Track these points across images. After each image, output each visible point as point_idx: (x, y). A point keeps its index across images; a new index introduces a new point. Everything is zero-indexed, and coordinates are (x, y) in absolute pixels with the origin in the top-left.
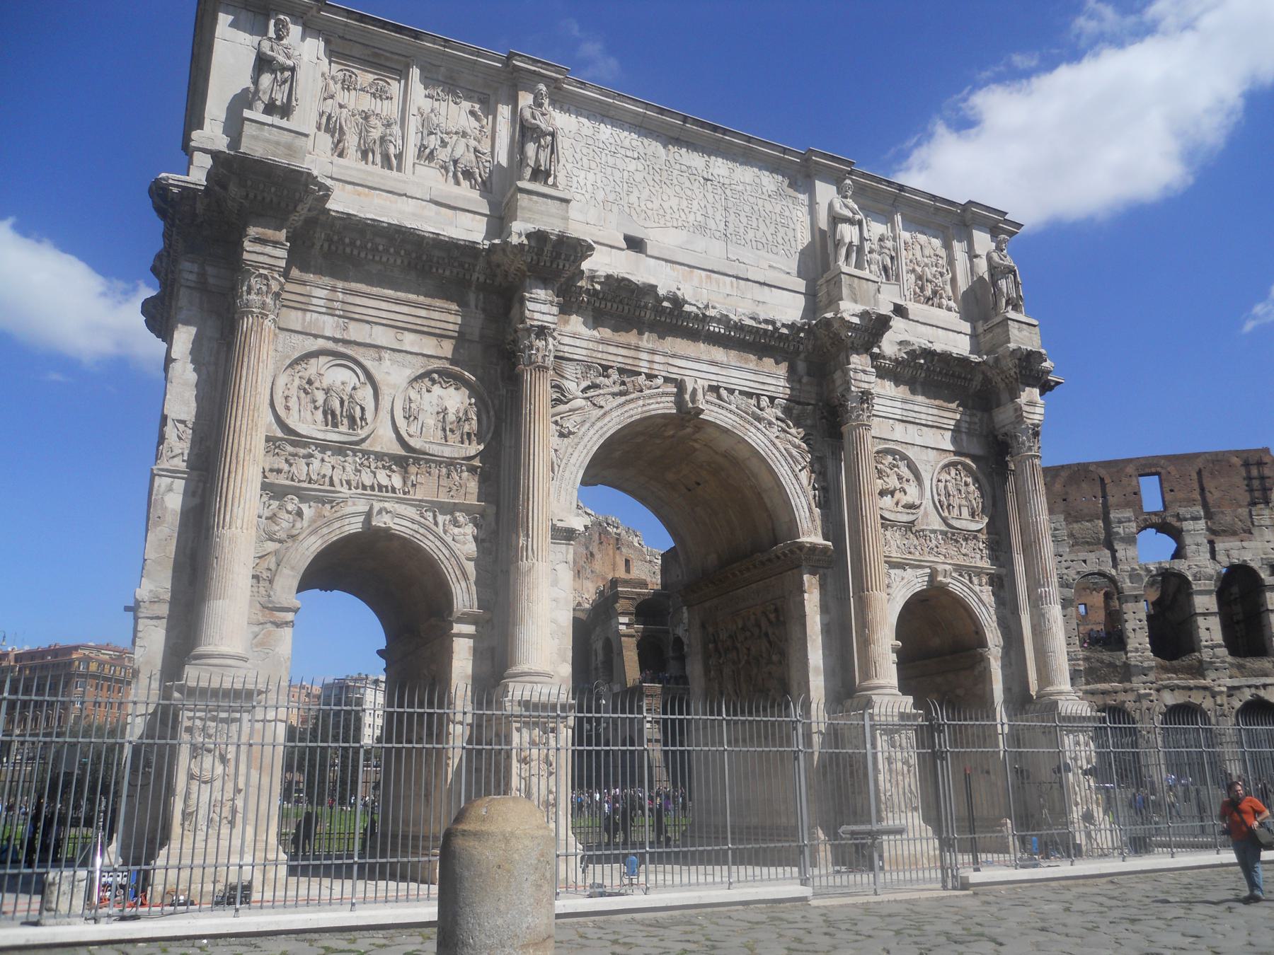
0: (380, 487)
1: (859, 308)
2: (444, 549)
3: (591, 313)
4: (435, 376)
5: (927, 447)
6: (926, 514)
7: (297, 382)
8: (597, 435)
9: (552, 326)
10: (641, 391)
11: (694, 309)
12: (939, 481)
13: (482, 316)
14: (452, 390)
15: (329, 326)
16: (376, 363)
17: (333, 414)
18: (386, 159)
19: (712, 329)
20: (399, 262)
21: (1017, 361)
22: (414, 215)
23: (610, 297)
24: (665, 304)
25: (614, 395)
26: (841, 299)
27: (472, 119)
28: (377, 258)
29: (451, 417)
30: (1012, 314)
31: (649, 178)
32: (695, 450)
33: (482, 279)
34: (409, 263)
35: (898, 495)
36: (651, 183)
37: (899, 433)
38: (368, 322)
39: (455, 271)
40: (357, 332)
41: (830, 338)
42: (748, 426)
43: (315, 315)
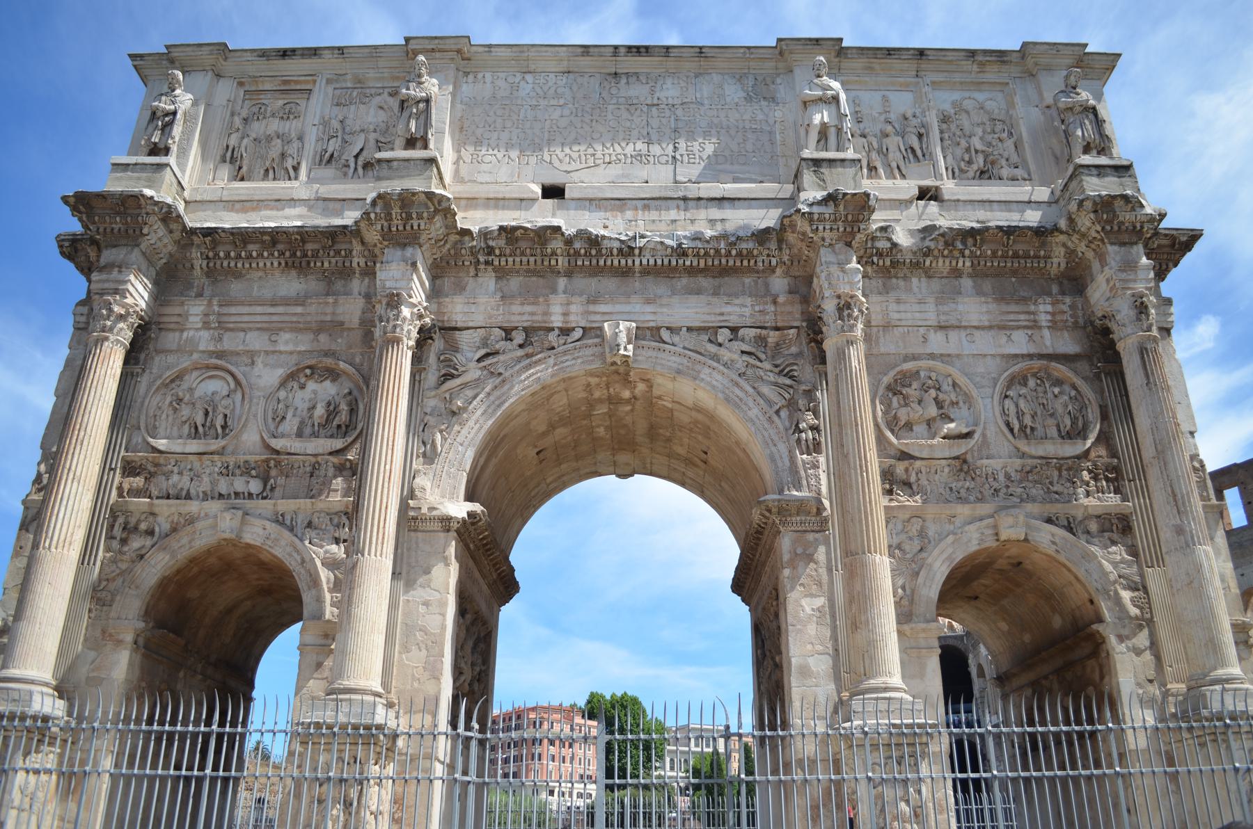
0: (237, 494)
1: (819, 195)
2: (295, 555)
3: (494, 274)
4: (308, 371)
5: (985, 355)
7: (169, 399)
8: (493, 407)
10: (553, 348)
11: (616, 245)
12: (1006, 397)
13: (364, 300)
14: (327, 383)
15: (204, 340)
16: (248, 369)
17: (196, 428)
19: (645, 262)
20: (276, 264)
21: (1092, 216)
23: (508, 251)
24: (577, 245)
25: (519, 360)
27: (381, 112)
28: (254, 265)
29: (320, 411)
30: (1087, 159)
32: (672, 410)
33: (362, 264)
34: (286, 263)
36: (579, 125)
37: (937, 342)
38: (243, 330)
39: (333, 260)
40: (230, 342)
41: (802, 240)
42: (698, 367)
43: (191, 333)
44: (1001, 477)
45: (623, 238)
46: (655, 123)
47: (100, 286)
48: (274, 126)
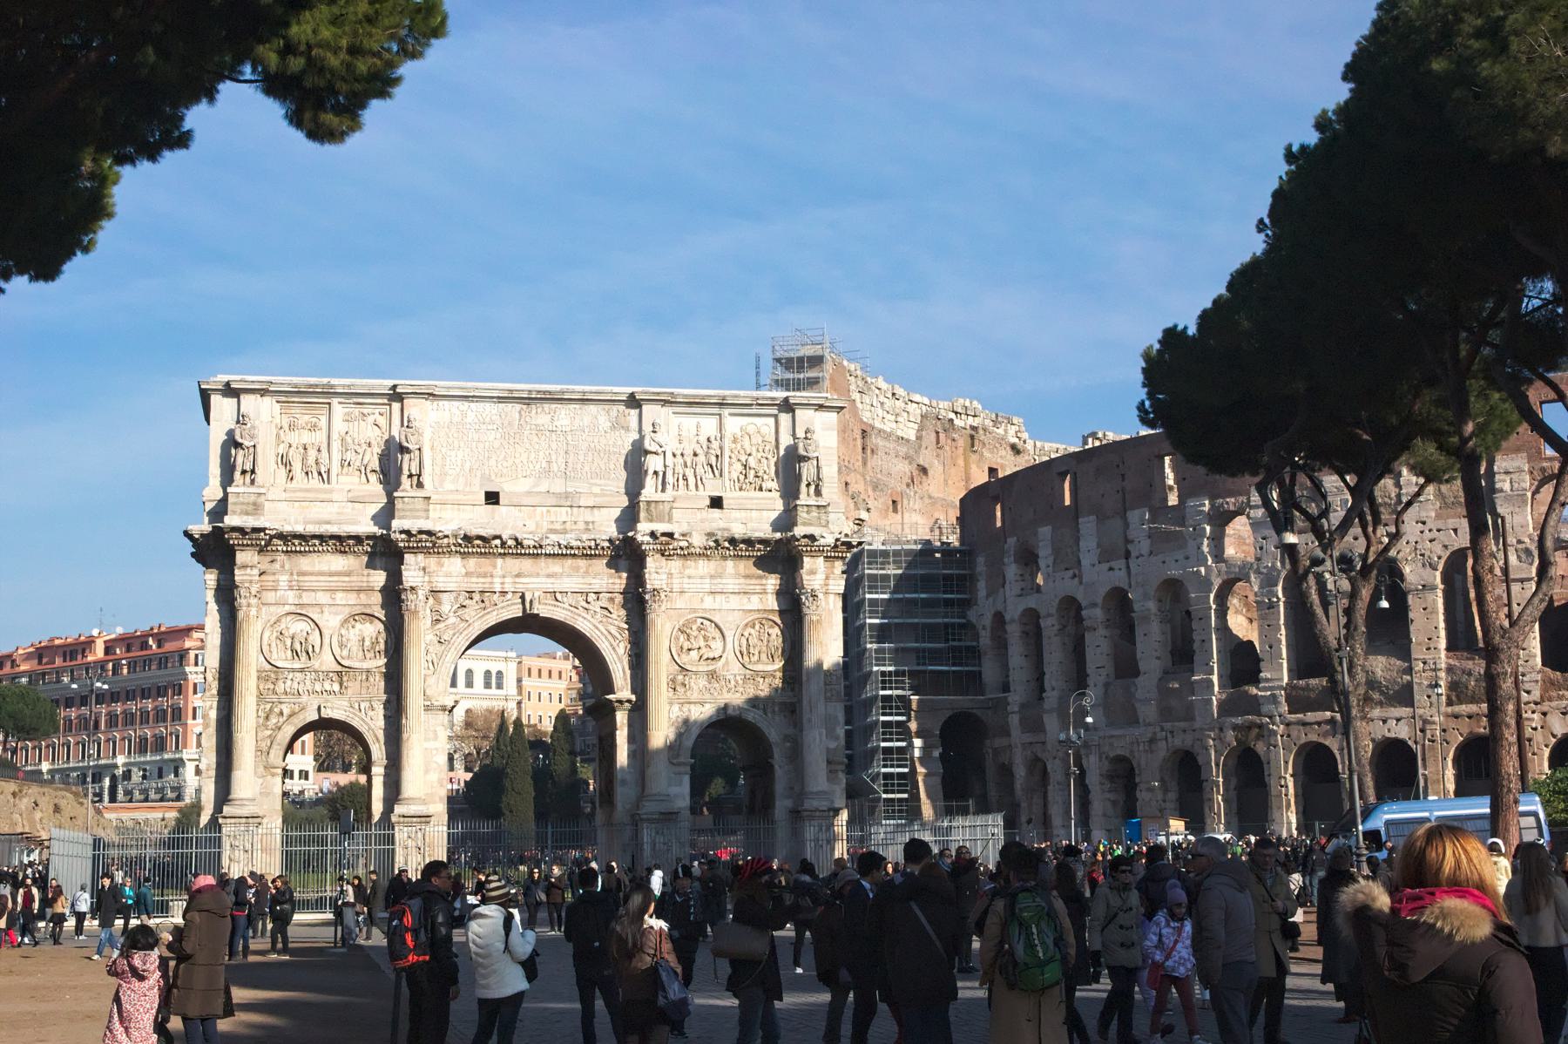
4: (356, 618)
6: (727, 662)
7: (275, 634)
9: (420, 584)
11: (532, 543)
14: (368, 624)
15: (291, 597)
18: (320, 474)
22: (338, 513)
24: (511, 542)
26: (639, 521)
29: (367, 643)
31: (505, 443)
35: (703, 651)
37: (709, 602)
38: (313, 590)
40: (307, 598)
42: (576, 617)
43: (282, 592)
44: (733, 682)
45: (537, 539)
46: (554, 446)
47: (240, 578)
48: (306, 437)
